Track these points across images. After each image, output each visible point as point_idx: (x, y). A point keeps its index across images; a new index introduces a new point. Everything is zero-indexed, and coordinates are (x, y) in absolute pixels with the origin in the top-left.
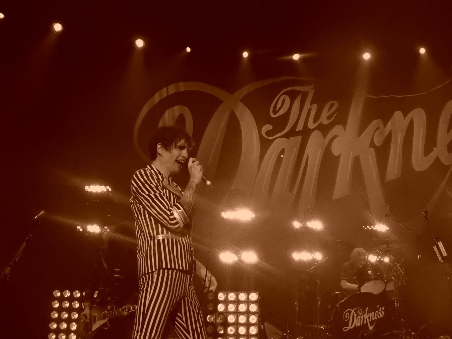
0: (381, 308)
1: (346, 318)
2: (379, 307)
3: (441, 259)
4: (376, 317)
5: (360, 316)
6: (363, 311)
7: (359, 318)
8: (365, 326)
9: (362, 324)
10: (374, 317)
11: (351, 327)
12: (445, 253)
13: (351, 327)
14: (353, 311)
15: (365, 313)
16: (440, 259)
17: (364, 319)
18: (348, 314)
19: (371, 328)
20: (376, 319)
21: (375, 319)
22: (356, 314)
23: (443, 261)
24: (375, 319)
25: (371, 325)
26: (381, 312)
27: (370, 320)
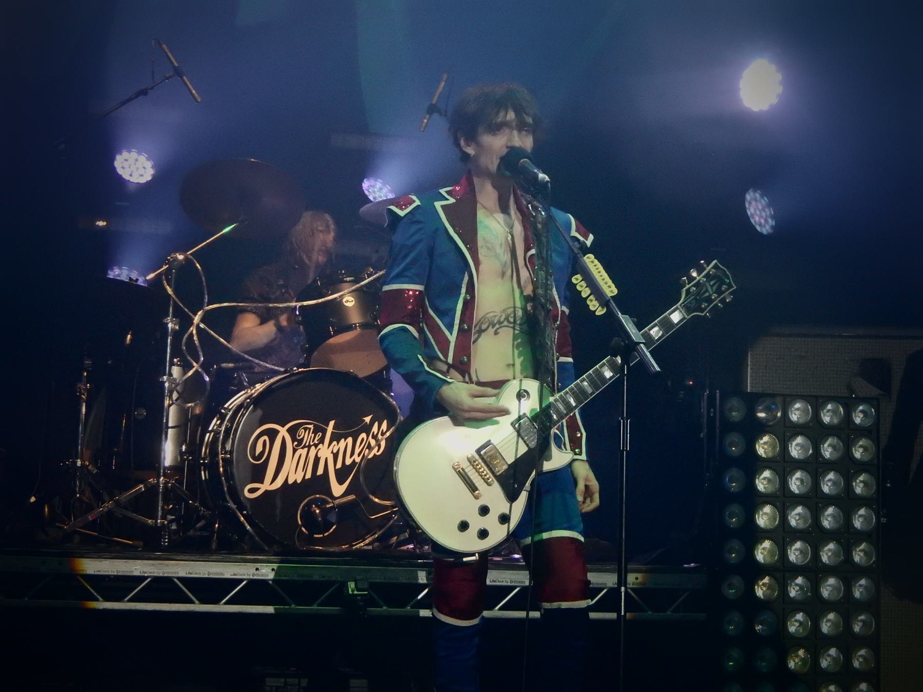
0: (376, 423)
1: (256, 455)
3: (598, 305)
4: (359, 456)
5: (306, 449)
6: (315, 432)
7: (301, 455)
8: (319, 483)
9: (308, 476)
10: (351, 457)
11: (271, 483)
12: (609, 287)
13: (271, 483)
14: (283, 431)
15: (322, 441)
16: (594, 306)
17: (317, 460)
18: (265, 442)
19: (338, 489)
20: (358, 460)
21: (354, 460)
23: (605, 310)
24: (354, 460)
25: (341, 481)
26: (374, 437)
27: (339, 465)
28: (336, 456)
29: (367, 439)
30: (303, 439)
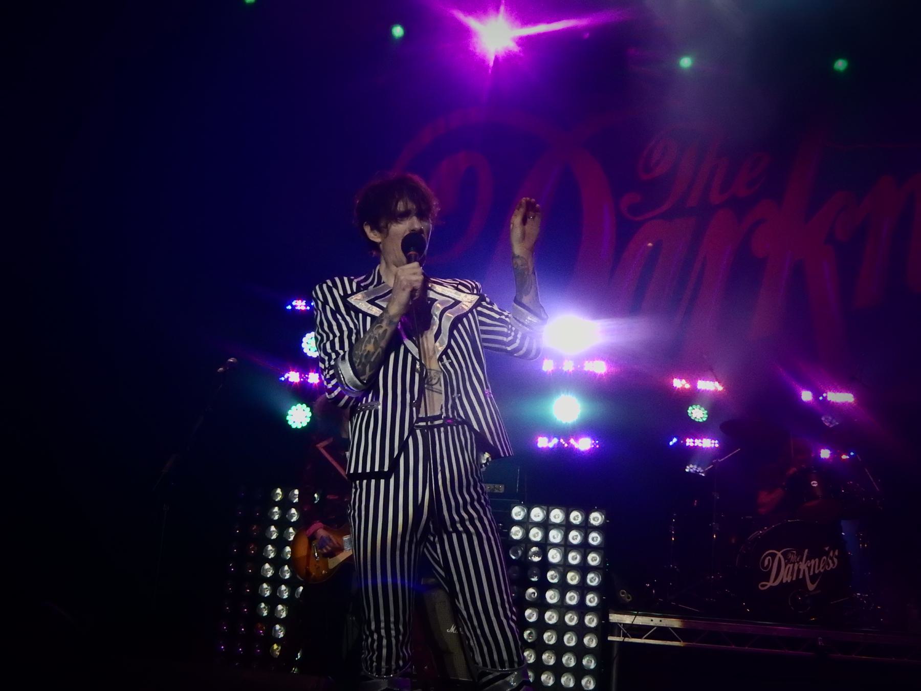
1: (765, 566)
2: (829, 549)
4: (823, 568)
7: (789, 568)
8: (798, 584)
9: (794, 579)
11: (774, 582)
13: (774, 582)
14: (779, 554)
15: (801, 560)
17: (799, 570)
18: (769, 559)
19: (811, 587)
20: (822, 571)
22: (785, 561)
25: (813, 583)
26: (831, 558)
27: (811, 573)
28: (809, 568)
29: (827, 559)
30: (791, 558)
